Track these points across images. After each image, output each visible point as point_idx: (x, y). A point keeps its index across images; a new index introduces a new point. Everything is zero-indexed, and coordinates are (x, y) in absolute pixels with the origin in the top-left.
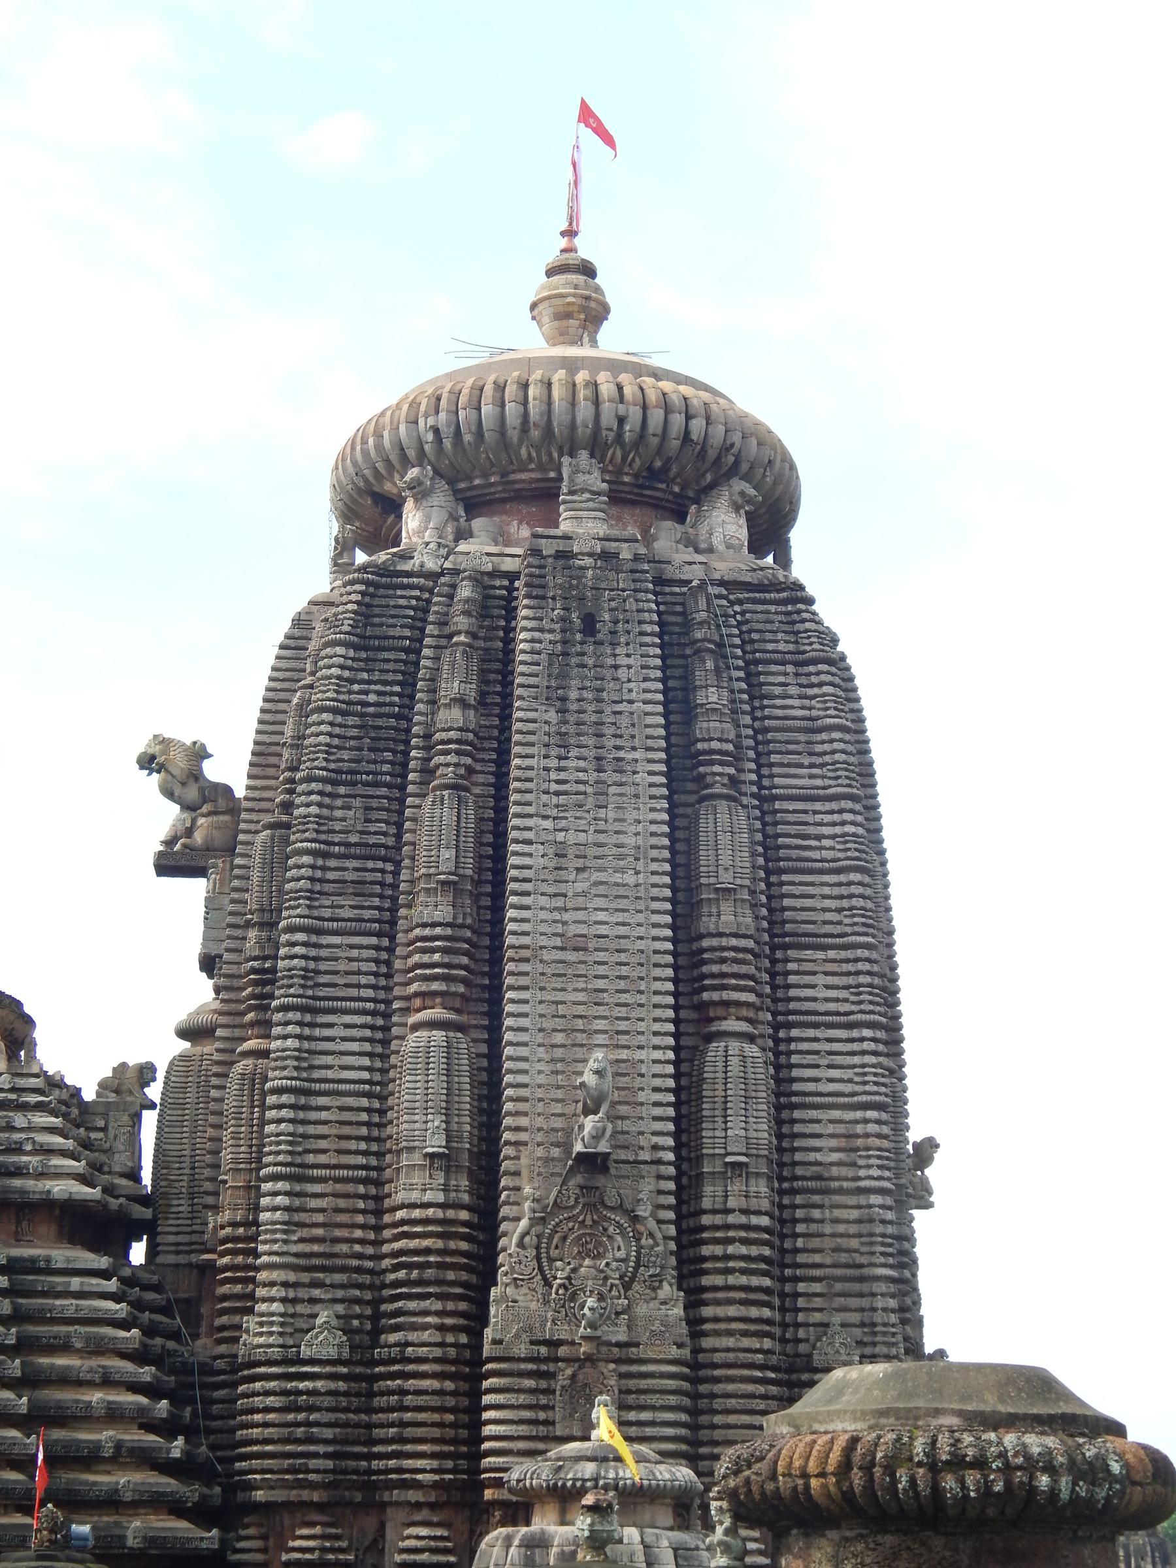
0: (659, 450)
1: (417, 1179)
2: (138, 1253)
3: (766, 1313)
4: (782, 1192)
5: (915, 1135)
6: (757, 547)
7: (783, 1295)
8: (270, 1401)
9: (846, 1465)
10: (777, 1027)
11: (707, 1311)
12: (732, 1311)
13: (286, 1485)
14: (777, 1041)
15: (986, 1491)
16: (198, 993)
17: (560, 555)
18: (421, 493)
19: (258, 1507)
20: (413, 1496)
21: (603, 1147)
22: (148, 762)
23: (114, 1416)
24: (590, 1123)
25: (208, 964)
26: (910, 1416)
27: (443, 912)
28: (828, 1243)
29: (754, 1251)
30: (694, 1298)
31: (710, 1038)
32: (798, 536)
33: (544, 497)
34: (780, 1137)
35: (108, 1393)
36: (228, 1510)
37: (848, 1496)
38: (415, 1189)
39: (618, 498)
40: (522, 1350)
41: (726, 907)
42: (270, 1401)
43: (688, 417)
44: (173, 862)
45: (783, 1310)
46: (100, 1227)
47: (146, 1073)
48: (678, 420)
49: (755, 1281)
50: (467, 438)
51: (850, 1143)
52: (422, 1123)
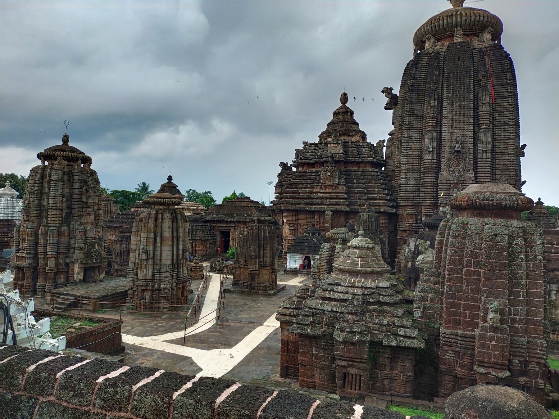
0: (474, 24)
1: (427, 155)
2: (383, 169)
3: (489, 175)
4: (493, 155)
5: (521, 144)
6: (493, 40)
7: (493, 172)
8: (404, 190)
9: (467, 201)
10: (493, 127)
11: (478, 175)
12: (483, 175)
13: (405, 203)
14: (493, 129)
15: (493, 204)
16: (393, 128)
17: (454, 47)
18: (429, 40)
19: (402, 206)
20: (426, 204)
21: (459, 149)
22: (383, 92)
23: (379, 193)
24: (457, 145)
25: (393, 123)
26: (481, 193)
27: (432, 111)
28: (502, 163)
29: (487, 165)
30: (476, 173)
31: (480, 130)
32: (502, 37)
33: (452, 36)
34: (493, 145)
35: (377, 189)
36: (397, 207)
37: (469, 205)
38: (427, 157)
39: (464, 35)
40: (444, 182)
41: (484, 107)
42: (404, 190)
43: (480, 16)
44: (386, 108)
45: (493, 174)
46: (377, 165)
47: (384, 141)
48: (477, 18)
49: (487, 170)
50: (437, 28)
51: (507, 146)
52: (427, 147)
